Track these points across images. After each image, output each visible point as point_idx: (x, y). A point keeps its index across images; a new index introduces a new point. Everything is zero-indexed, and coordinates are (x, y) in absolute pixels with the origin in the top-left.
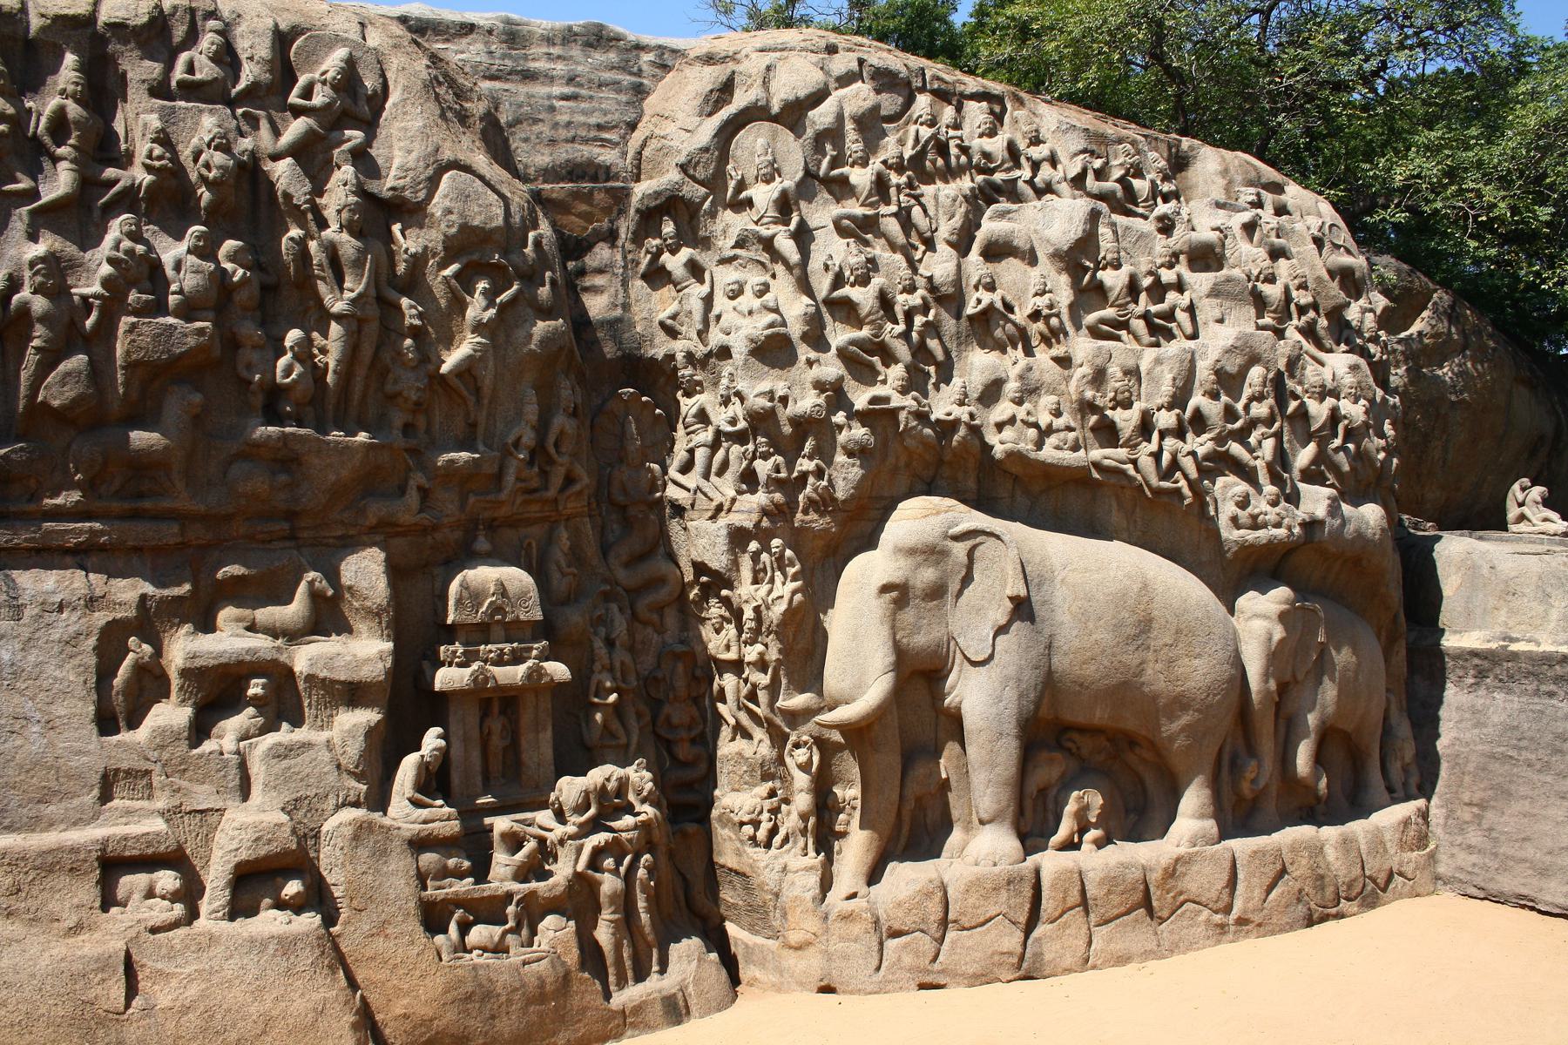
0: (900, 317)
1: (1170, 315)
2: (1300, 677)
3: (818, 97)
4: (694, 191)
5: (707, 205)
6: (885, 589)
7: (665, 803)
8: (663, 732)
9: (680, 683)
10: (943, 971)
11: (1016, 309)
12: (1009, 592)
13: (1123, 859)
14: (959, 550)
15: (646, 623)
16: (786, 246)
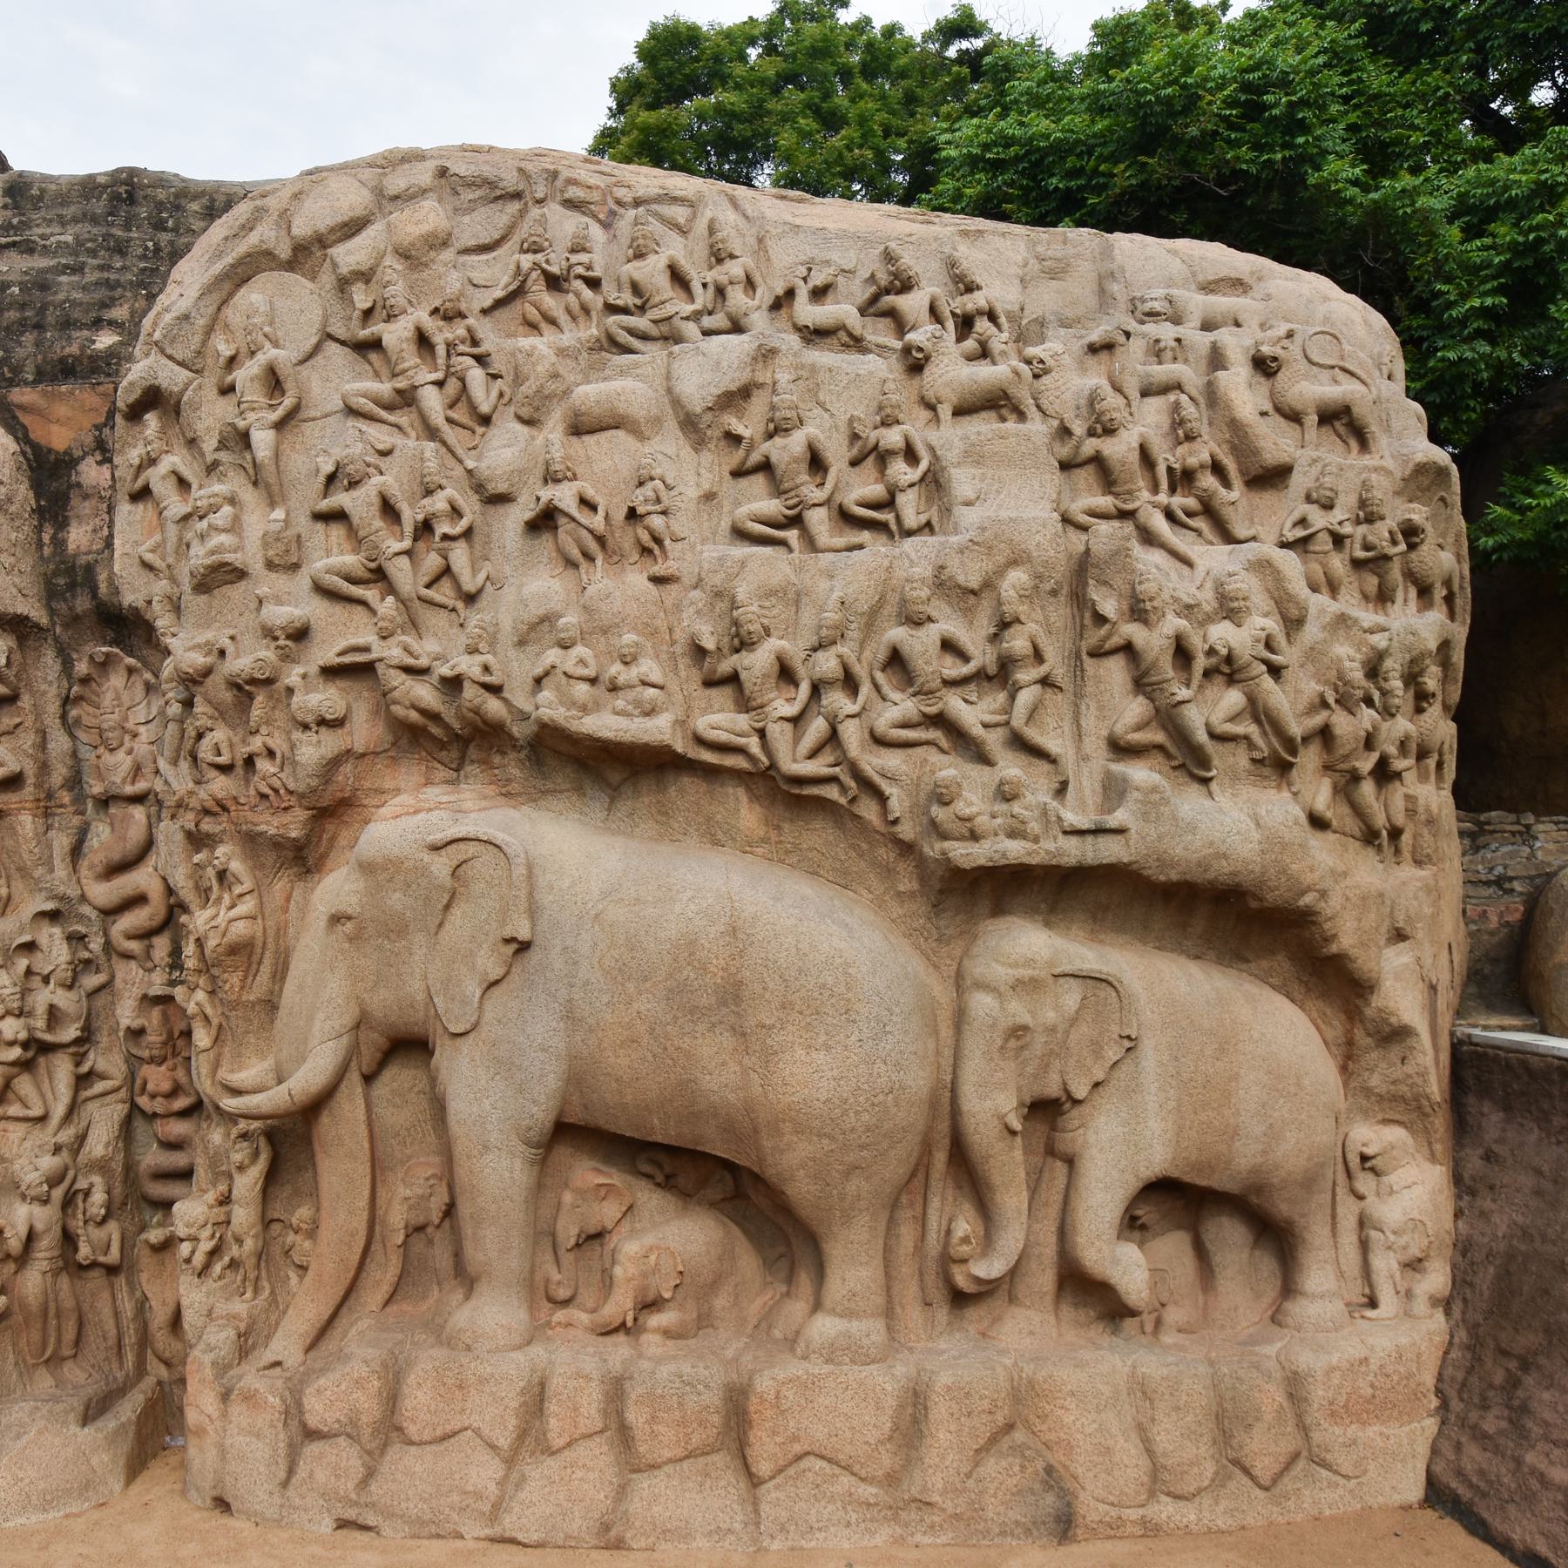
0: (408, 528)
1: (889, 503)
2: (1080, 1091)
3: (352, 228)
4: (171, 377)
5: (189, 392)
6: (337, 919)
7: (98, 1197)
8: (143, 1101)
9: (154, 1038)
10: (372, 1505)
11: (600, 509)
12: (508, 933)
13: (686, 1369)
14: (441, 866)
15: (128, 956)
16: (263, 440)
